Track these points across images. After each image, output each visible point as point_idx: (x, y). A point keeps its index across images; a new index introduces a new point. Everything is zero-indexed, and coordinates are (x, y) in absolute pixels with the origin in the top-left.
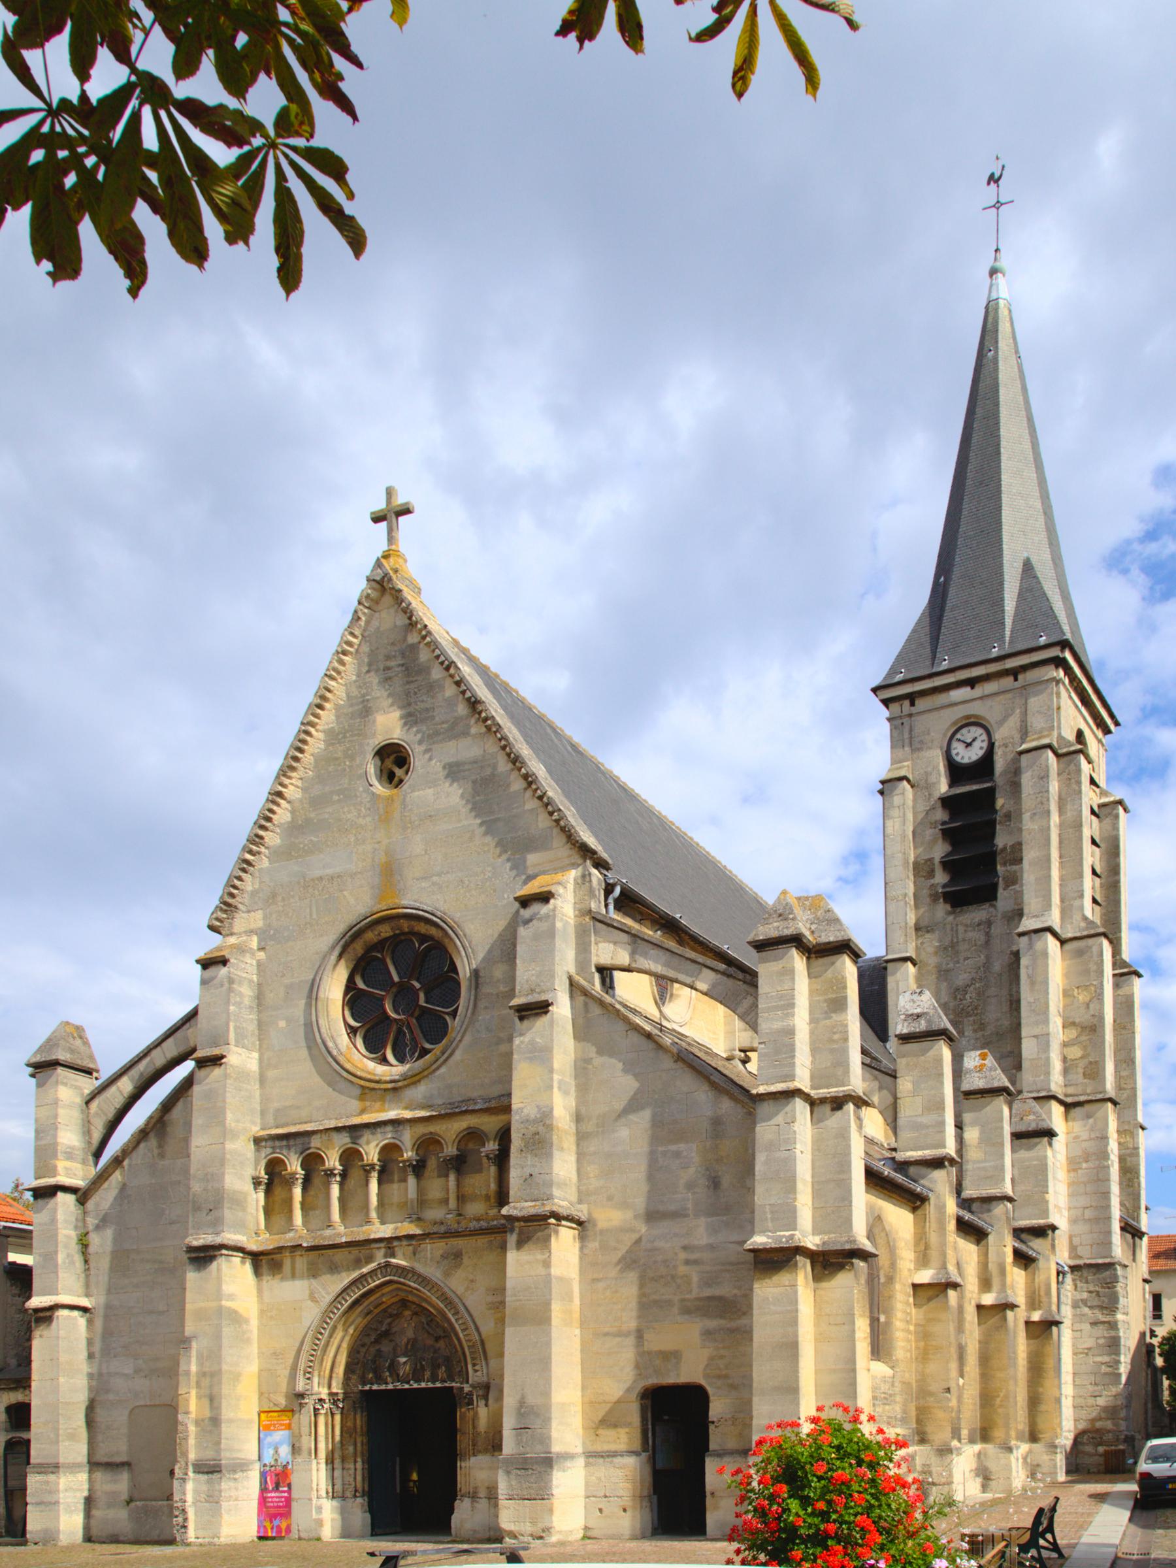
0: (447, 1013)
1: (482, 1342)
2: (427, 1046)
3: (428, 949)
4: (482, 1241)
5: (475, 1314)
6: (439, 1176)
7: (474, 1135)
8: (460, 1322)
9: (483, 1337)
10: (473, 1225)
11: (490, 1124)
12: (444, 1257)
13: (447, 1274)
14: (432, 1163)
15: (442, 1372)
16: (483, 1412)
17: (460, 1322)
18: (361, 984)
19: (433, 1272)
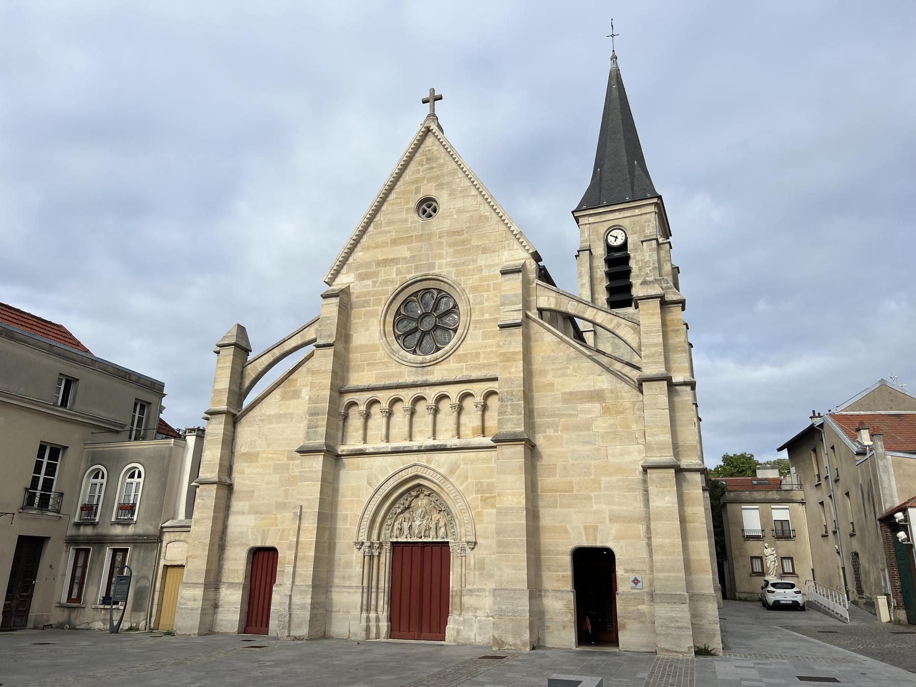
0: (451, 329)
18: (403, 312)
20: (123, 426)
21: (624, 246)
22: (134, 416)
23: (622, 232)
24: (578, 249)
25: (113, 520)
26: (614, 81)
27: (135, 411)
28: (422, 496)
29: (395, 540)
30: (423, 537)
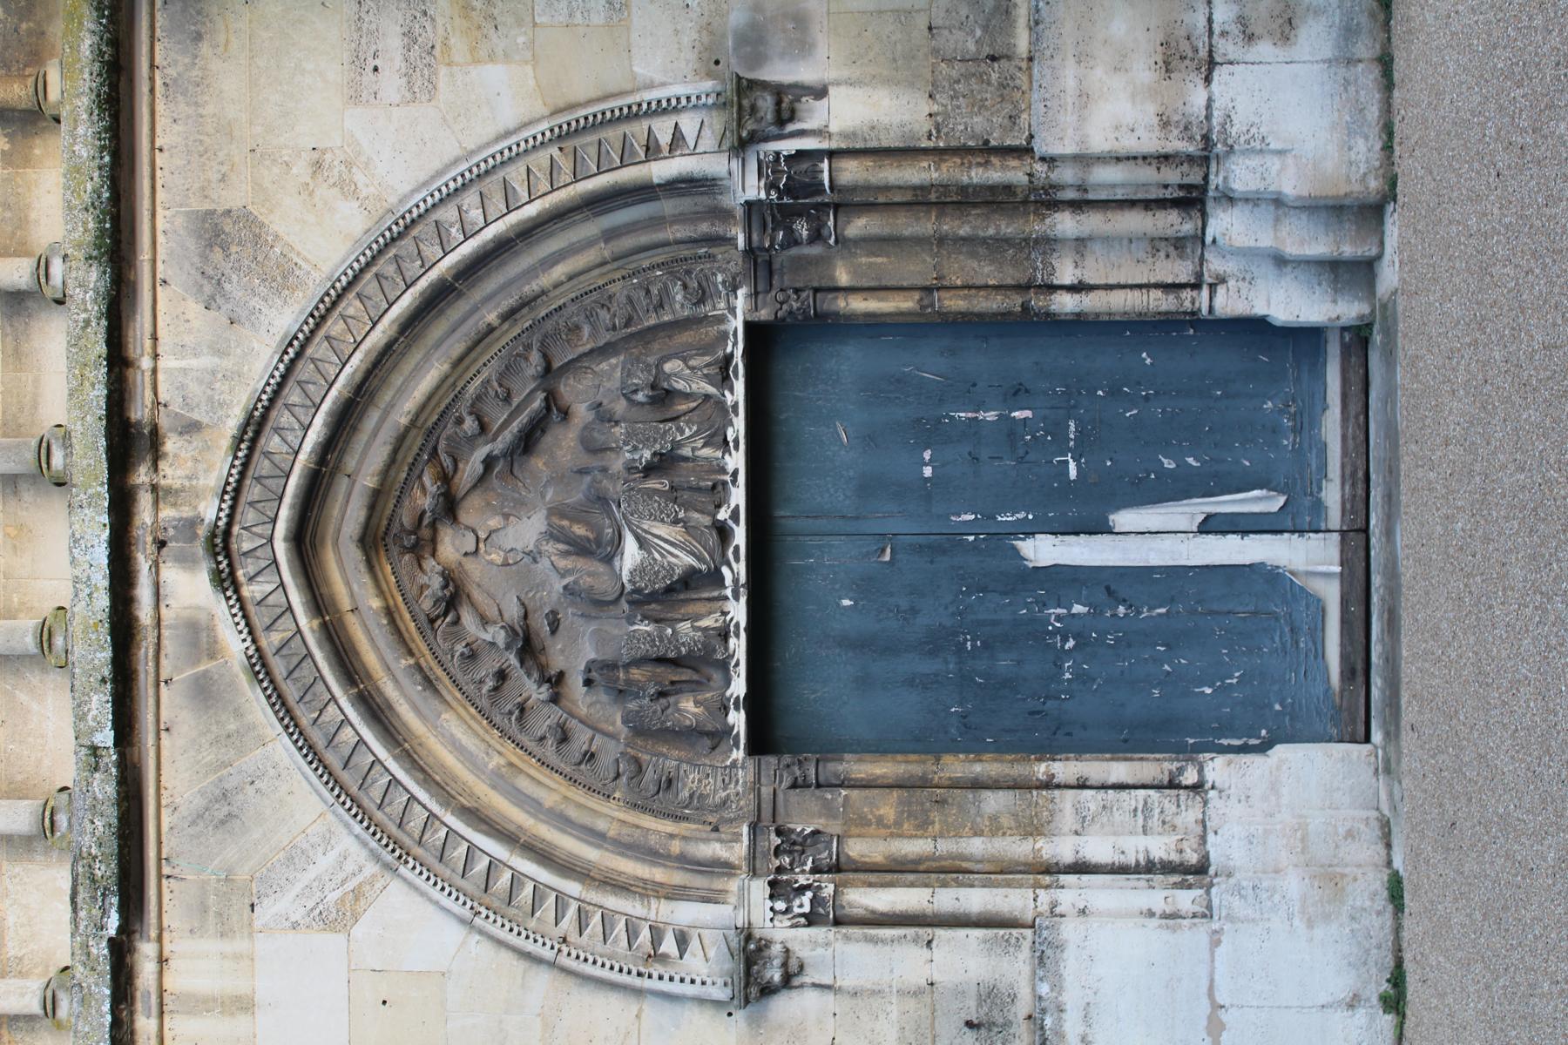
8: (475, 215)
9: (542, 110)
12: (213, 292)
13: (283, 278)
17: (475, 215)
29: (737, 720)
30: (723, 515)
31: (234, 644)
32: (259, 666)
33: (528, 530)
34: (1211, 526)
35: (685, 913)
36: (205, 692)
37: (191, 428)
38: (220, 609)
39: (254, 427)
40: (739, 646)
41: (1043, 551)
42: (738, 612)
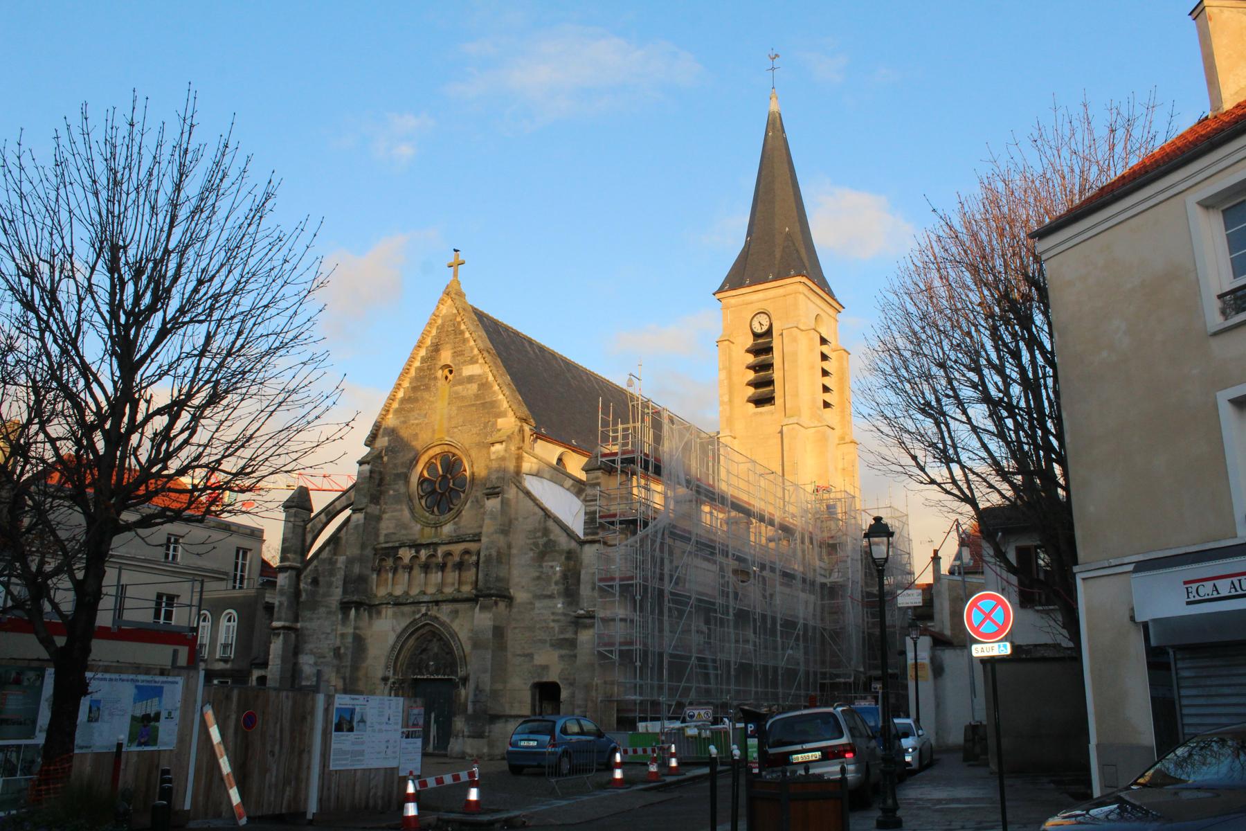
1: (465, 657)
2: (452, 506)
3: (456, 460)
4: (467, 605)
5: (463, 642)
6: (453, 571)
7: (467, 552)
10: (465, 596)
11: (473, 546)
12: (451, 612)
13: (452, 621)
14: (450, 564)
15: (448, 670)
16: (463, 692)
19: (444, 617)
20: (226, 574)
21: (769, 333)
22: (237, 564)
23: (766, 316)
24: (717, 340)
25: (217, 657)
26: (771, 126)
27: (237, 557)
28: (435, 640)
31: (417, 616)
32: (415, 620)
33: (436, 650)
34: (434, 737)
35: (392, 672)
36: (414, 612)
37: (438, 610)
38: (420, 615)
39: (436, 618)
40: (422, 677)
41: (433, 716)
42: (425, 677)
